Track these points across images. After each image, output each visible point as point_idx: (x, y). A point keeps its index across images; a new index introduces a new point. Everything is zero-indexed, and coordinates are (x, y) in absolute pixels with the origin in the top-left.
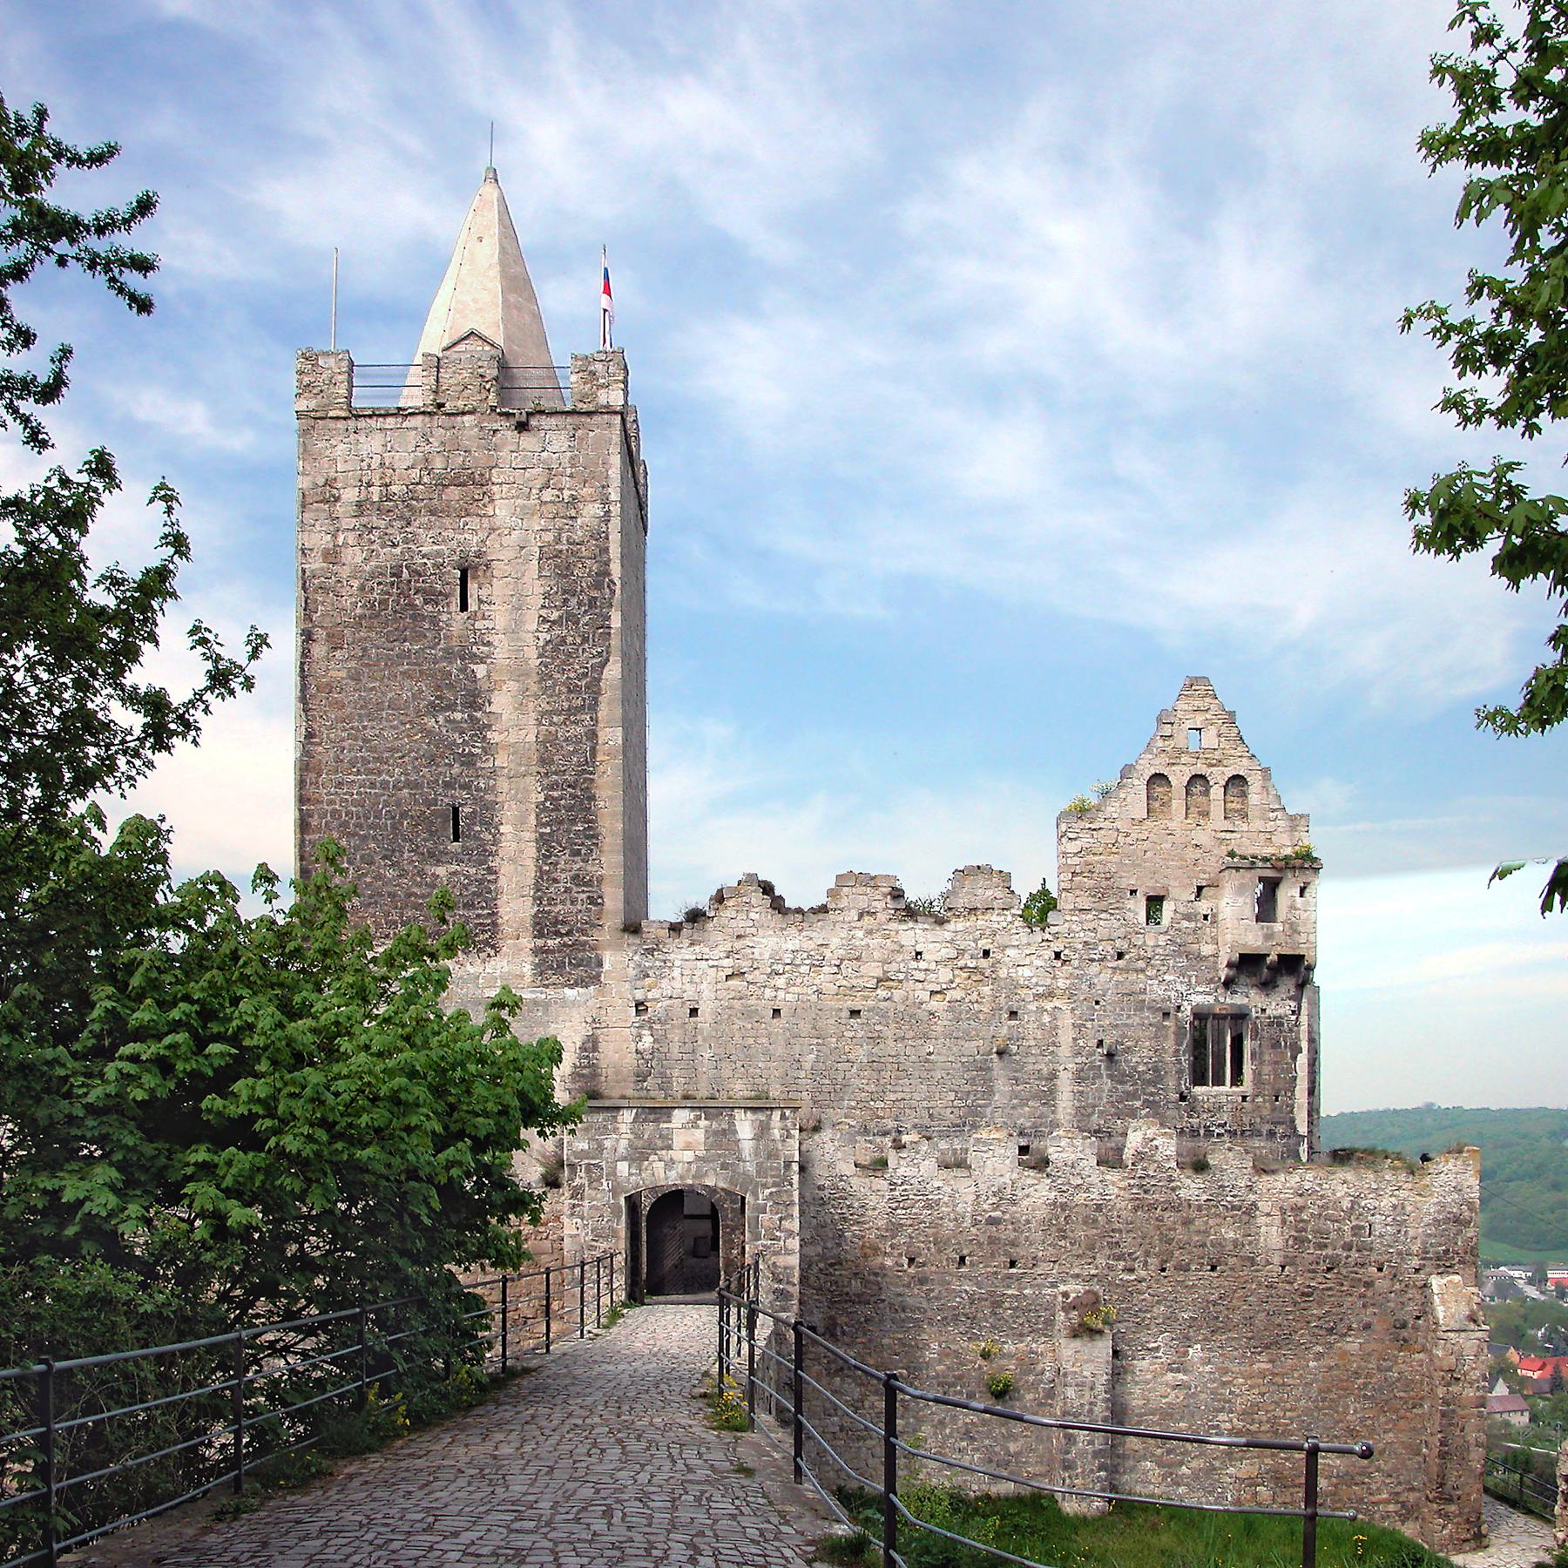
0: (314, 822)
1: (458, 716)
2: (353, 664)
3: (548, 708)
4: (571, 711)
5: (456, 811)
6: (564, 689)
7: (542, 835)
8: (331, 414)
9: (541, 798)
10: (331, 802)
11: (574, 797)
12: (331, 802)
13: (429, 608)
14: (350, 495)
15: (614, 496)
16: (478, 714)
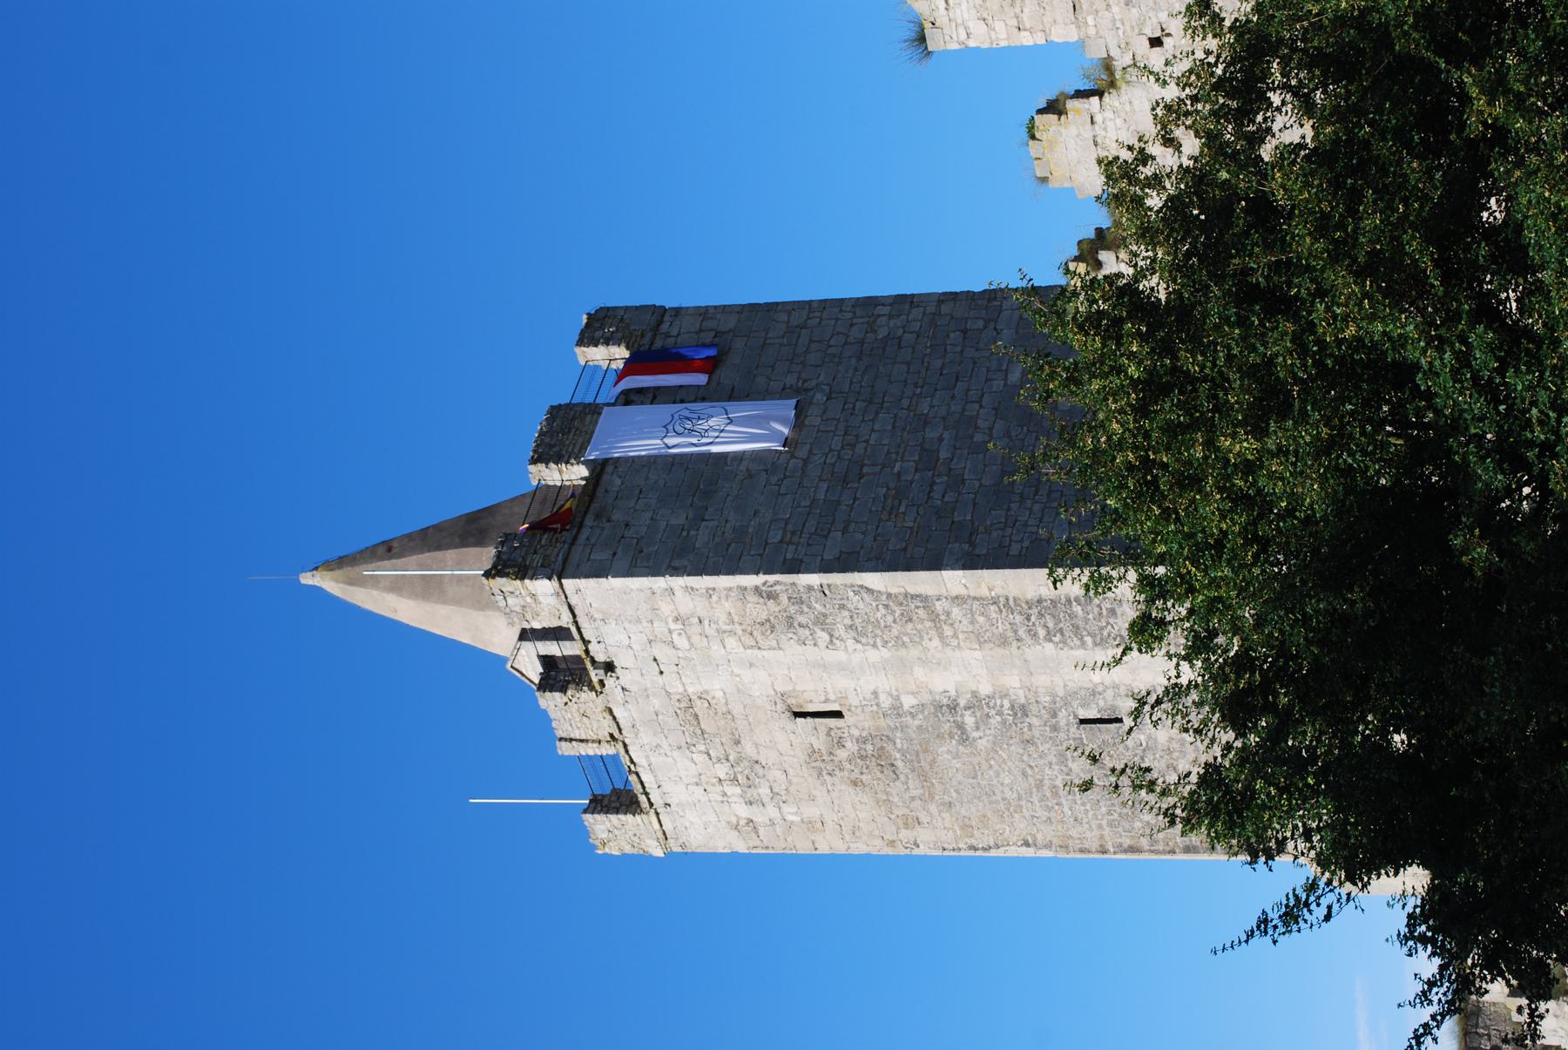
0: (1127, 842)
1: (969, 720)
2: (933, 808)
3: (936, 642)
4: (934, 617)
5: (1083, 721)
6: (910, 625)
7: (1095, 644)
8: (657, 826)
9: (1049, 646)
10: (1100, 827)
11: (1041, 615)
12: (1100, 827)
13: (848, 744)
14: (743, 811)
15: (660, 583)
16: (962, 703)
